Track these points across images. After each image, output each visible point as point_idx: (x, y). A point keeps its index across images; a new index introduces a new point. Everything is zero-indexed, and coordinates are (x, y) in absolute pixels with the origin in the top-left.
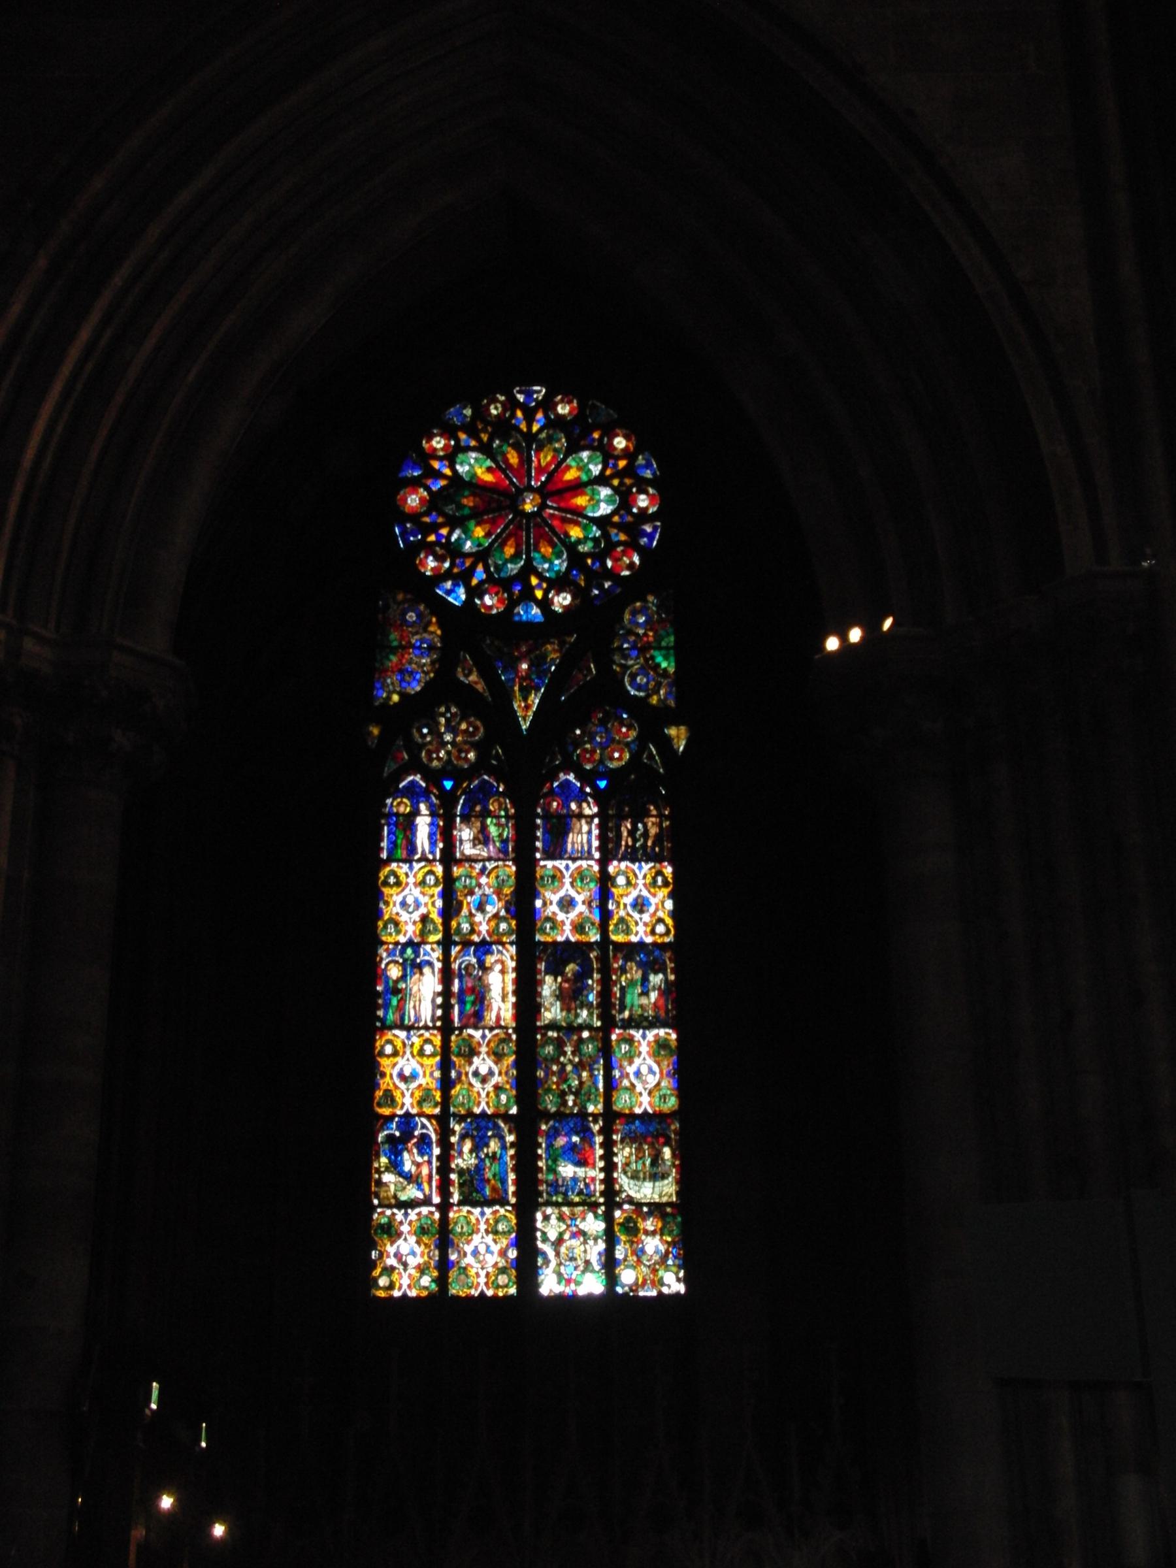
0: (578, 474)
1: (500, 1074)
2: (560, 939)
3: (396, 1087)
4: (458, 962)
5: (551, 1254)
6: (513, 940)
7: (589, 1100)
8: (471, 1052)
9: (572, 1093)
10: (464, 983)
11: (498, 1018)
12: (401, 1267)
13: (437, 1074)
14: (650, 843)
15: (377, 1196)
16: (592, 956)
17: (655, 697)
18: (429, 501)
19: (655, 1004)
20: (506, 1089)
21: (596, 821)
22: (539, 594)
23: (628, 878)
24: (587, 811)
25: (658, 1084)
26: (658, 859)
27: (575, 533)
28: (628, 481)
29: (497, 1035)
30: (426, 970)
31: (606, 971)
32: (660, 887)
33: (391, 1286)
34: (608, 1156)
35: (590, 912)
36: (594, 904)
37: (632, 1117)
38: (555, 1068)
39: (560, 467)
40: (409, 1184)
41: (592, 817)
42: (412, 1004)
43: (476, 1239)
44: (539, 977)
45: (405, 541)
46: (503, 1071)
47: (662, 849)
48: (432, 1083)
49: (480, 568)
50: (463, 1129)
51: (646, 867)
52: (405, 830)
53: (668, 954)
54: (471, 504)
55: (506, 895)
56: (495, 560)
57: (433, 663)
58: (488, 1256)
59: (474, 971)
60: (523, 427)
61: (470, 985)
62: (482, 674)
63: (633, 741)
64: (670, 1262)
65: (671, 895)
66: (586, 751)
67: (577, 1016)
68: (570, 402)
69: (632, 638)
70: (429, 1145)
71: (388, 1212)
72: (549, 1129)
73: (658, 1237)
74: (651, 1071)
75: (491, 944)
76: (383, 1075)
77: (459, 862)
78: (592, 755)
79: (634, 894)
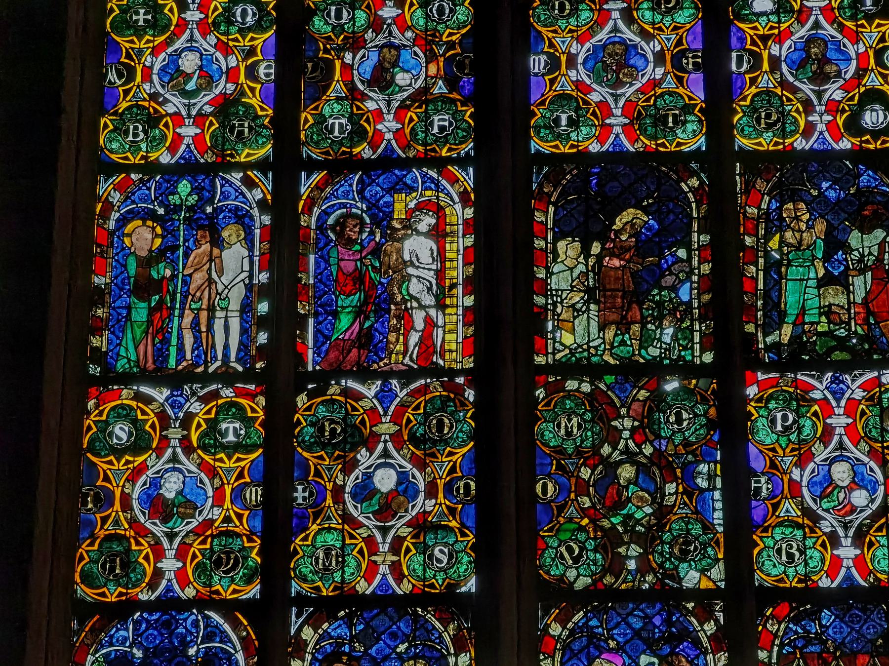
1: (431, 491)
3: (141, 531)
4: (316, 211)
6: (467, 153)
7: (684, 556)
9: (637, 538)
10: (332, 261)
13: (254, 495)
16: (686, 189)
19: (865, 299)
20: (451, 529)
29: (425, 389)
30: (231, 233)
32: (870, 18)
35: (680, 80)
38: (585, 473)
44: (539, 243)
46: (440, 483)
48: (240, 517)
55: (451, 45)
59: (361, 232)
61: (349, 267)
67: (645, 341)
72: (572, 632)
76: (104, 500)
79: (802, 32)
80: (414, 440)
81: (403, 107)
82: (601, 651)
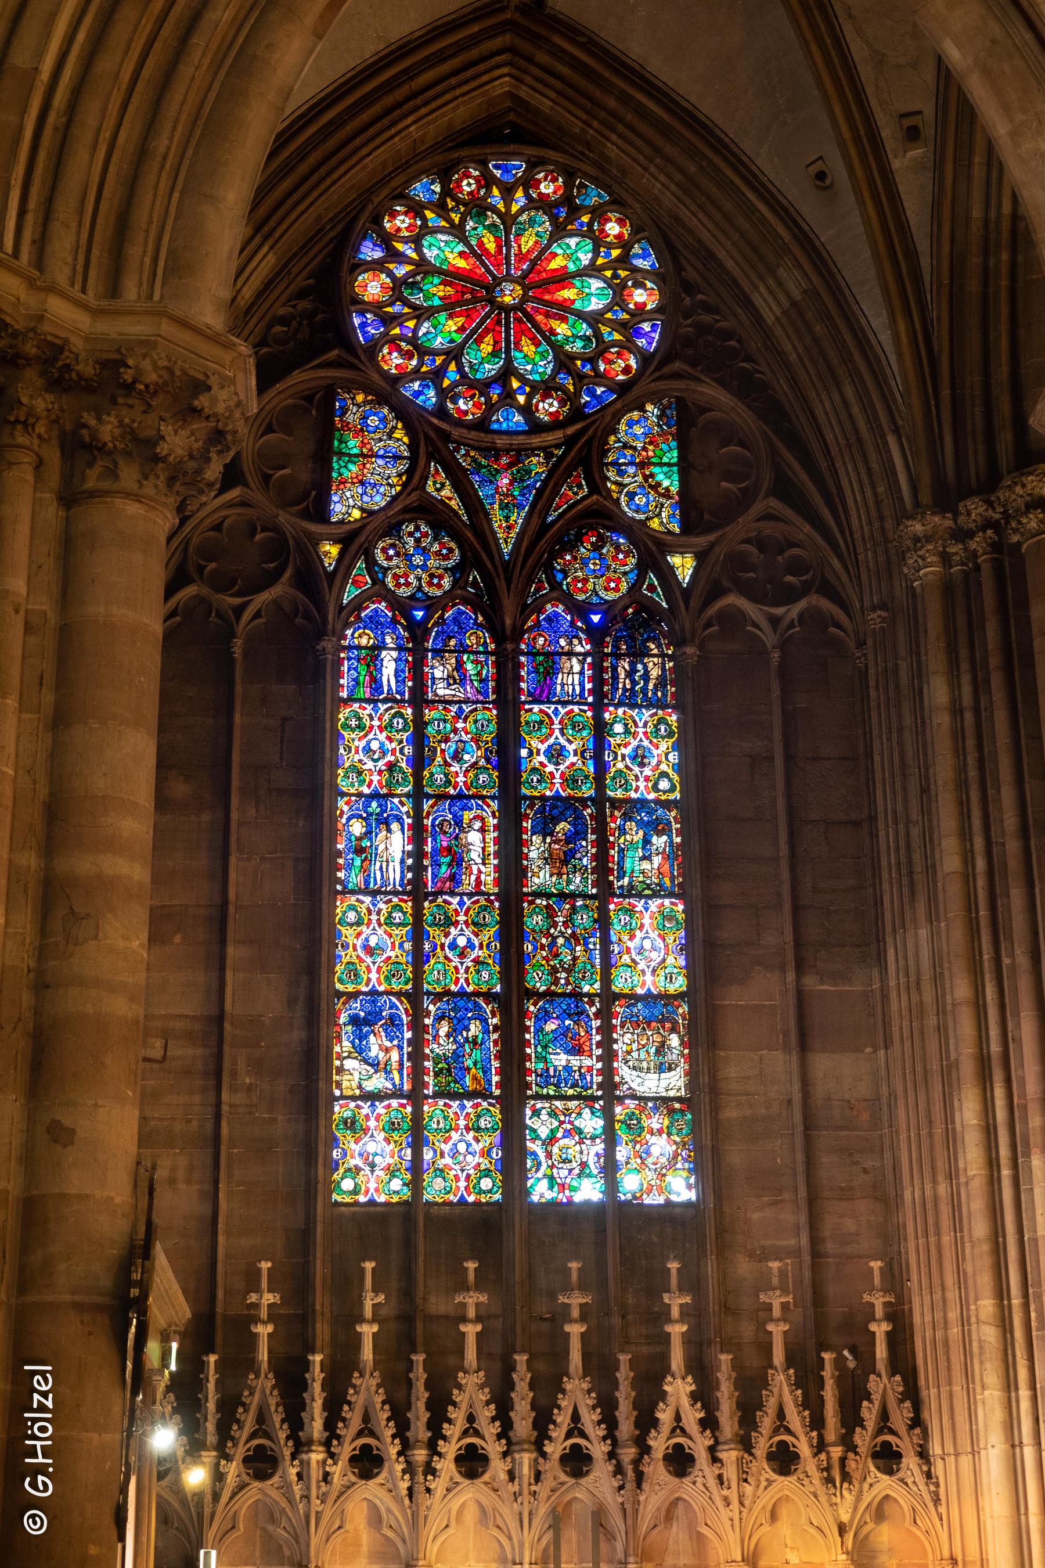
0: (563, 263)
1: (481, 947)
2: (548, 793)
3: (362, 961)
5: (542, 1156)
8: (450, 922)
9: (565, 970)
11: (478, 882)
12: (367, 1168)
13: (408, 946)
14: (651, 686)
15: (339, 1085)
17: (656, 520)
18: (393, 289)
21: (589, 660)
22: (521, 399)
23: (626, 725)
24: (579, 649)
25: (664, 960)
26: (661, 705)
27: (562, 329)
28: (623, 273)
29: (477, 901)
30: (395, 826)
31: (601, 829)
32: (663, 738)
33: (355, 1192)
34: (607, 1043)
36: (587, 755)
37: (632, 998)
38: (544, 941)
39: (544, 253)
40: (376, 1072)
41: (585, 655)
42: (378, 864)
43: (455, 1136)
45: (364, 333)
47: (664, 695)
49: (453, 366)
50: (439, 1009)
51: (646, 714)
52: (368, 666)
53: (673, 814)
54: (442, 294)
56: (471, 356)
57: (400, 475)
58: (469, 1158)
60: (501, 206)
61: (445, 844)
62: (456, 487)
63: (632, 570)
64: (679, 1166)
65: (676, 747)
66: (576, 580)
67: (569, 882)
68: (554, 180)
69: (629, 452)
70: (399, 1027)
71: (352, 1105)
73: (664, 1136)
74: (654, 948)
75: (469, 797)
76: (345, 946)
77: (431, 704)
78: (584, 585)
79: (635, 743)
80: (475, 924)
81: (467, 771)
82: (550, 1018)
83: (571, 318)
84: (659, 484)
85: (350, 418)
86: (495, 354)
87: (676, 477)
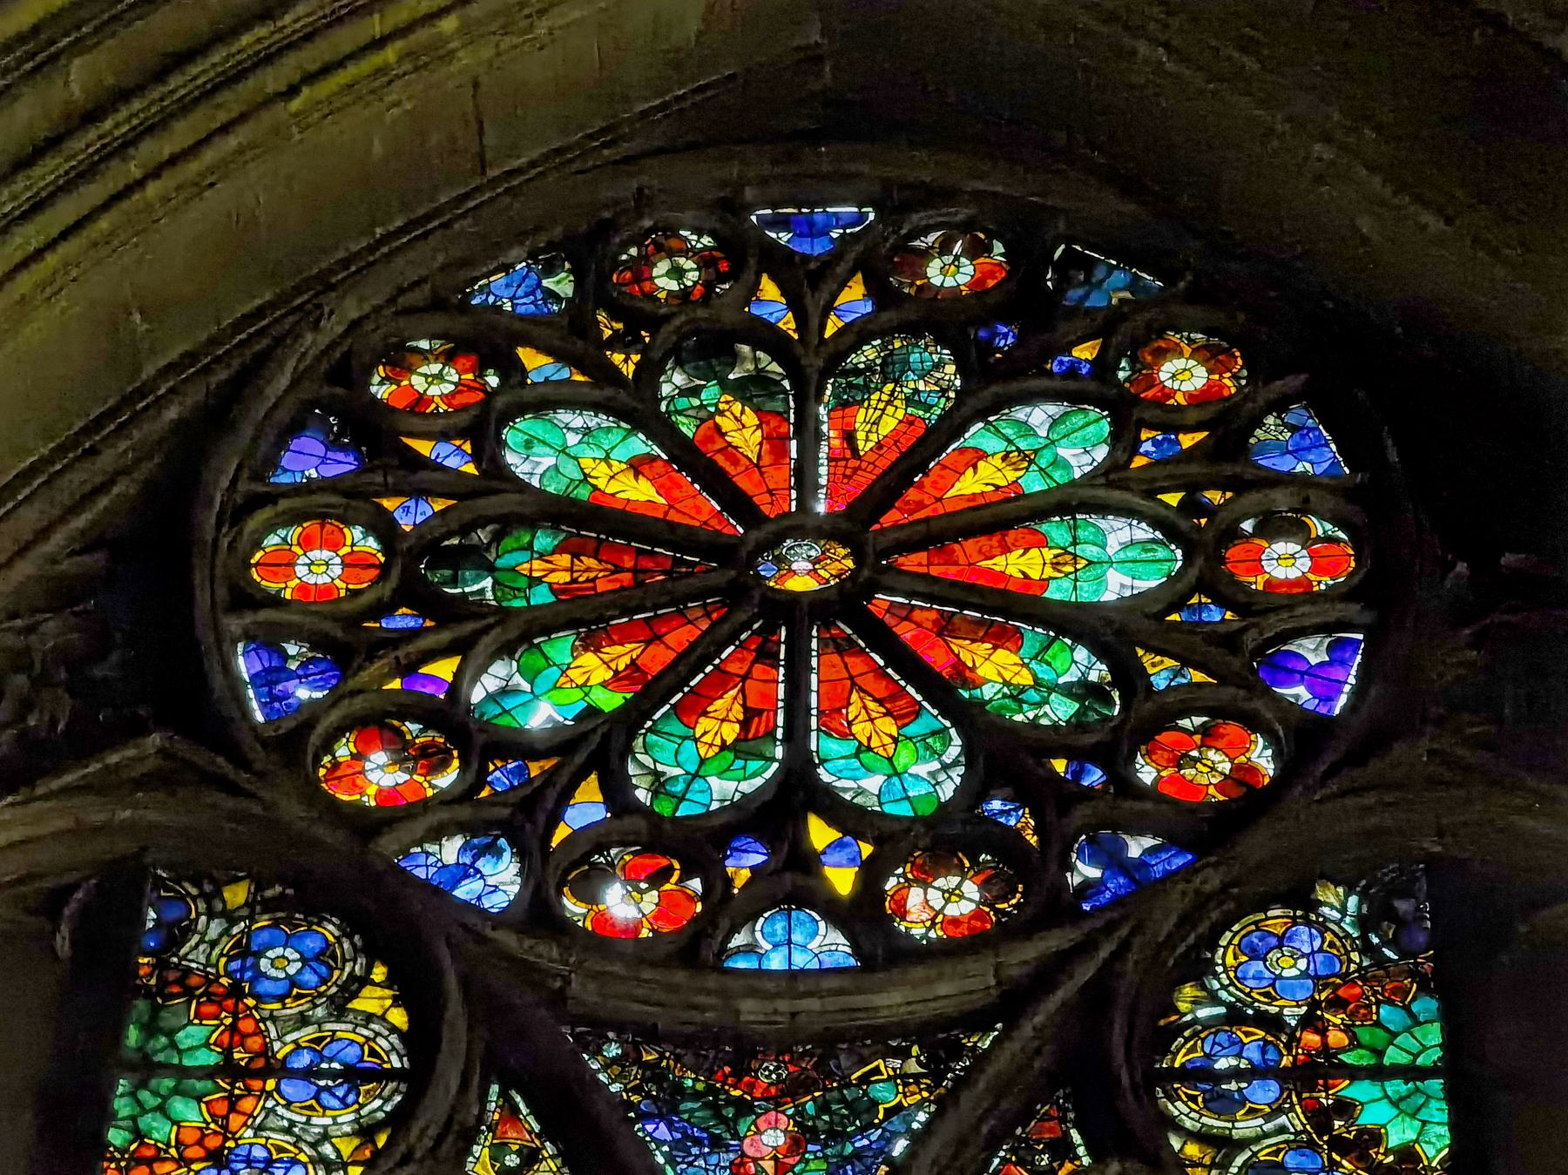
22: (842, 880)
45: (272, 700)
68: (976, 250)
83: (1034, 636)
84: (1374, 1137)
85: (194, 954)
86: (744, 747)
87: (1438, 1112)
